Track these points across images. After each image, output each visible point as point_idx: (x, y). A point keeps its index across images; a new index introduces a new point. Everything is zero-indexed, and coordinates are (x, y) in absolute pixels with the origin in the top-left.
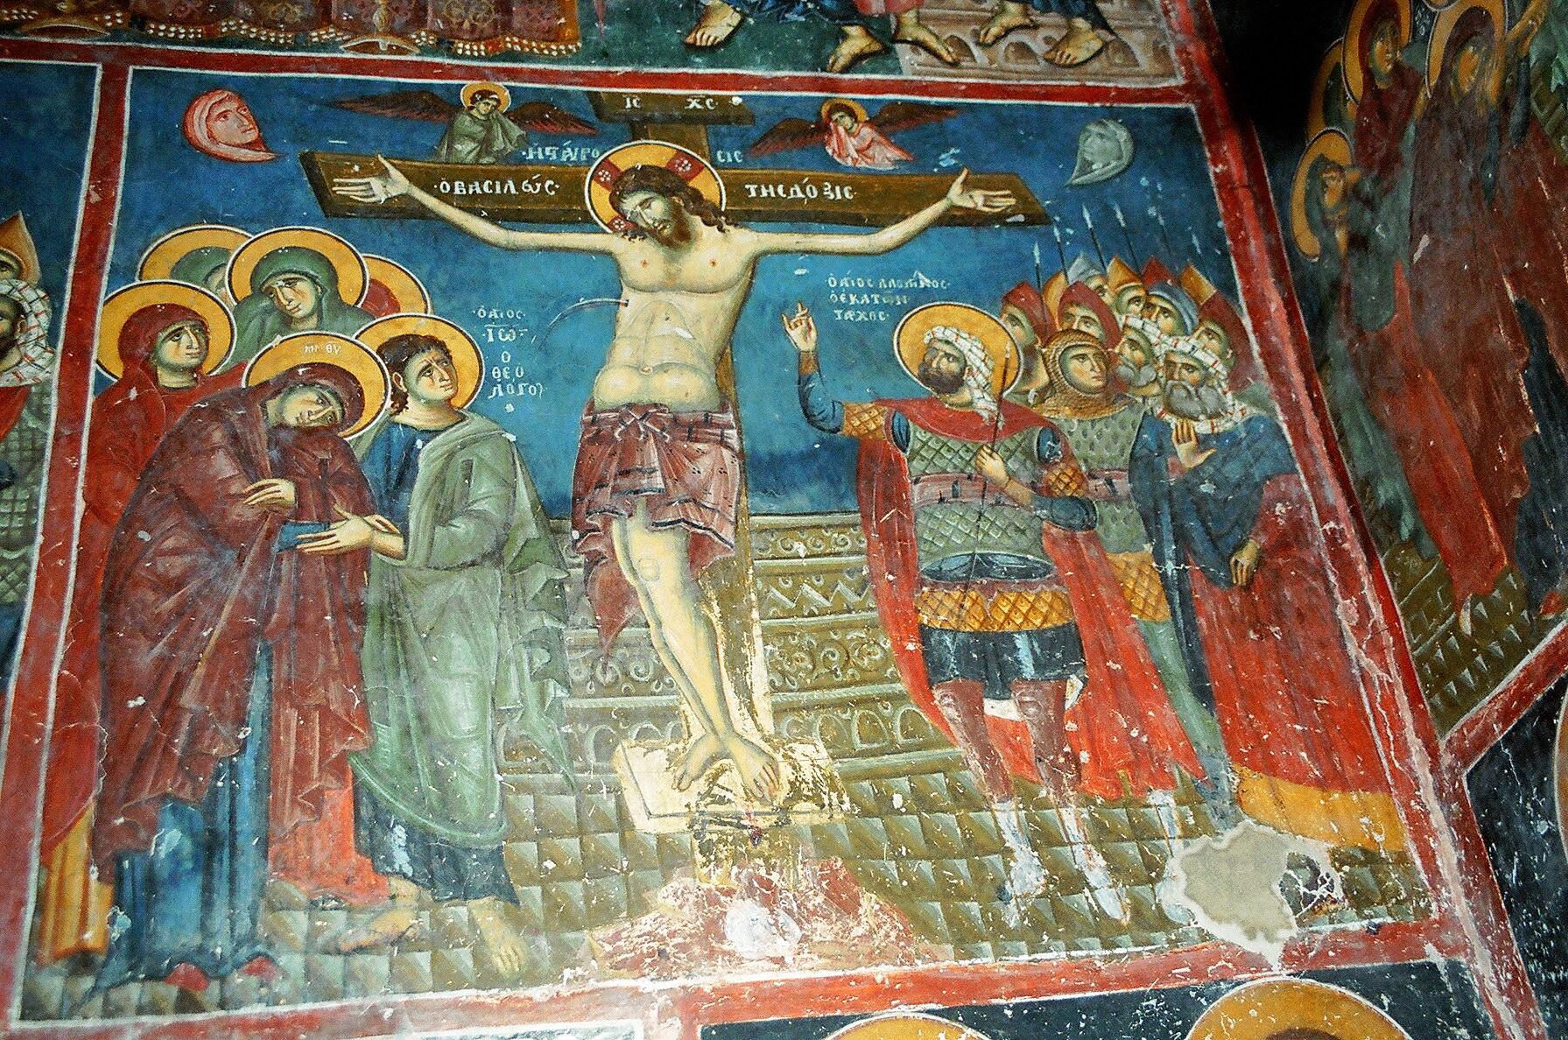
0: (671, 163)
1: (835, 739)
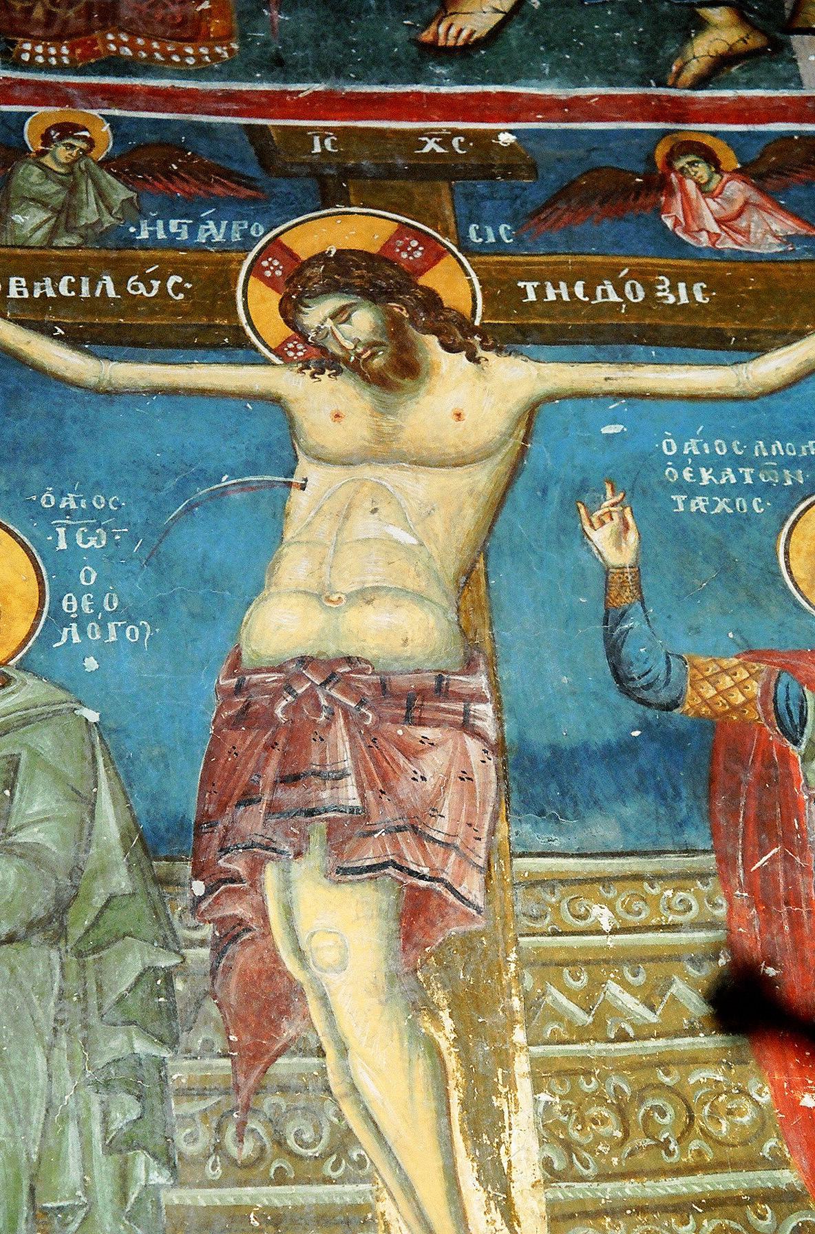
0: (388, 245)
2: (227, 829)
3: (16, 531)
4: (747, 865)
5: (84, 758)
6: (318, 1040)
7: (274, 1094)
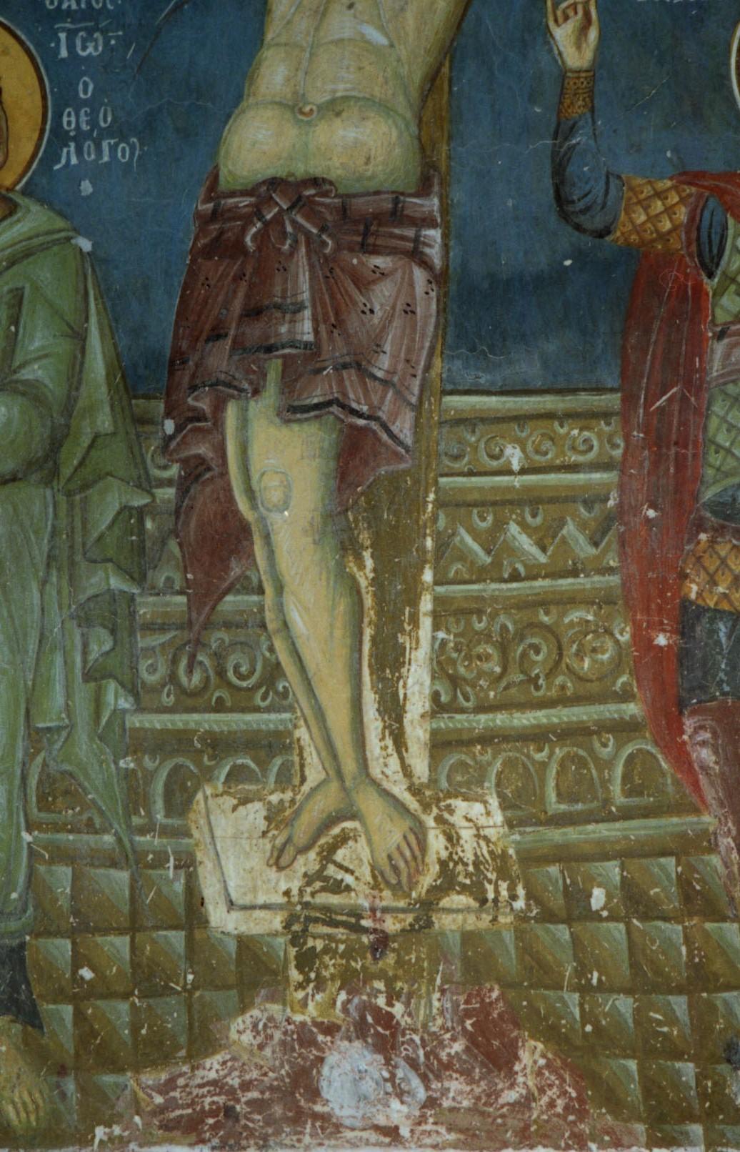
1: (518, 793)
2: (197, 366)
3: (23, 37)
4: (648, 405)
5: (77, 292)
6: (260, 581)
7: (219, 629)
